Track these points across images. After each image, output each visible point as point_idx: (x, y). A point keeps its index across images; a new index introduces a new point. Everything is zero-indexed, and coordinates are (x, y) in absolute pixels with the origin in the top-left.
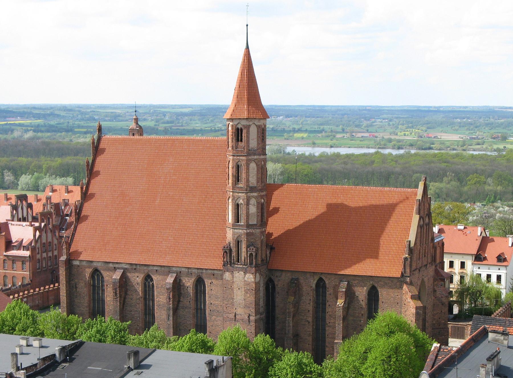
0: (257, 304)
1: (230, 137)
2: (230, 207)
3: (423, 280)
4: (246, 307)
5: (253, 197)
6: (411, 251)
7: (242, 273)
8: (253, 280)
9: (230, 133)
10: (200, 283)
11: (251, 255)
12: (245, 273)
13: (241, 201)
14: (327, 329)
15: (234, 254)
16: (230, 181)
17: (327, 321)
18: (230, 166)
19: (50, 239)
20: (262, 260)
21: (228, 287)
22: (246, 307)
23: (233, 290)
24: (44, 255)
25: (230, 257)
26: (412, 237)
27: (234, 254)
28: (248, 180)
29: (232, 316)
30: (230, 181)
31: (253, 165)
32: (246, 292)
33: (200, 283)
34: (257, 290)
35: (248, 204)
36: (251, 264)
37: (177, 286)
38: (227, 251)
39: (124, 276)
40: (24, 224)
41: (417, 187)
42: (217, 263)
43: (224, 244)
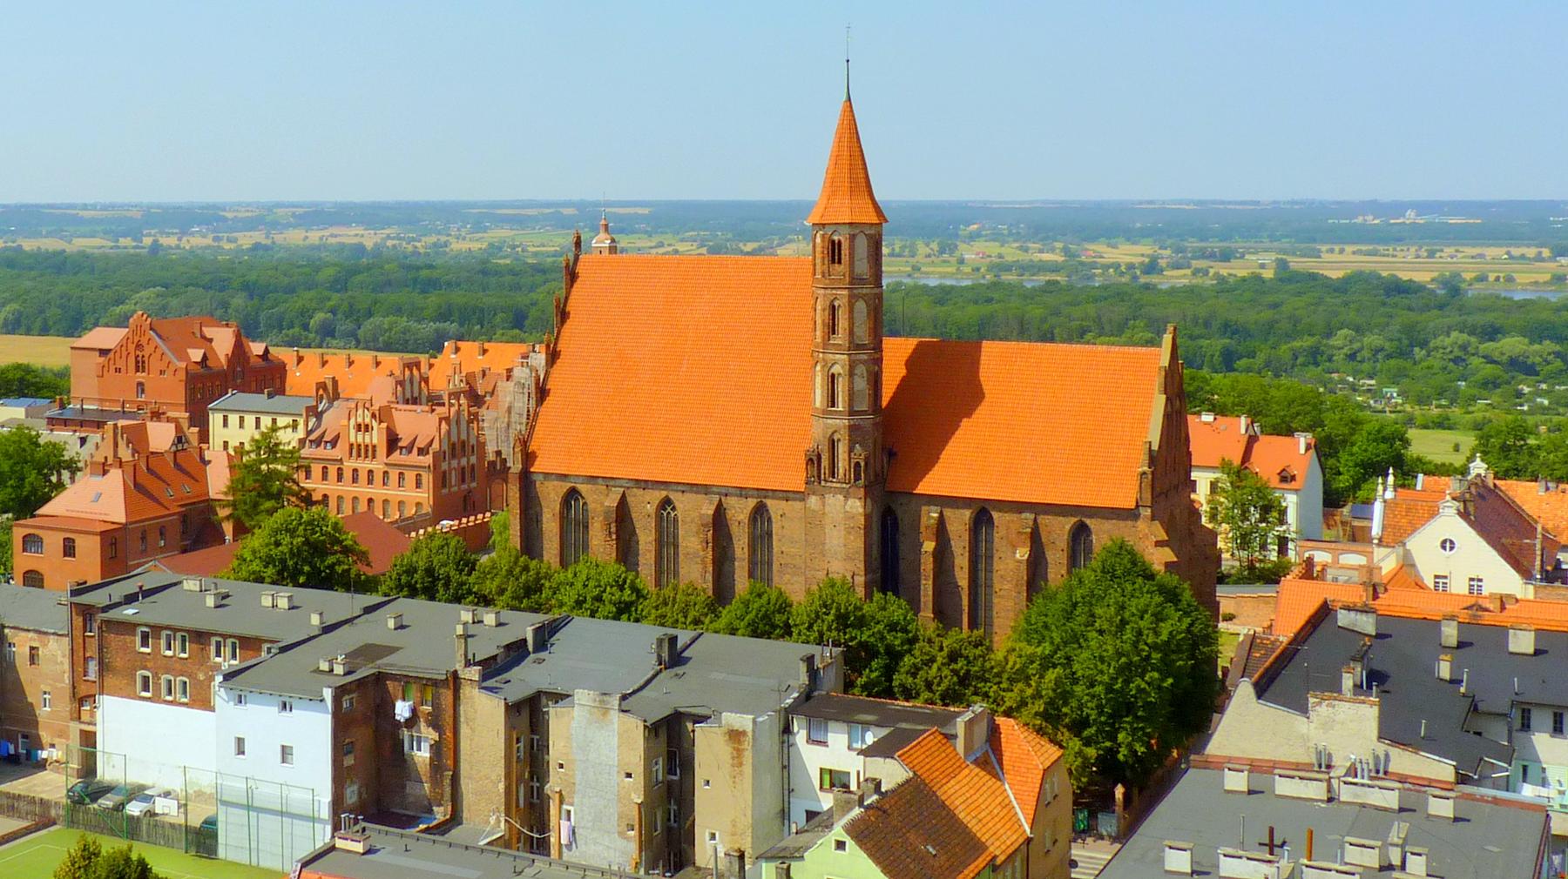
0: (867, 554)
1: (819, 255)
2: (819, 380)
3: (1172, 514)
4: (848, 558)
5: (861, 362)
6: (1153, 459)
7: (841, 497)
8: (861, 510)
9: (819, 249)
10: (760, 512)
11: (857, 464)
12: (846, 498)
13: (837, 369)
14: (995, 601)
15: (825, 463)
16: (818, 333)
17: (997, 587)
18: (819, 307)
19: (464, 437)
20: (876, 475)
21: (814, 523)
22: (848, 558)
23: (823, 528)
24: (454, 463)
25: (818, 466)
26: (1154, 436)
27: (825, 463)
28: (851, 333)
29: (821, 575)
30: (818, 333)
31: (861, 306)
32: (849, 530)
33: (760, 512)
34: (867, 528)
35: (851, 374)
36: (857, 478)
37: (719, 520)
38: (813, 460)
39: (623, 502)
40: (418, 408)
41: (1160, 345)
42: (796, 481)
43: (811, 445)
